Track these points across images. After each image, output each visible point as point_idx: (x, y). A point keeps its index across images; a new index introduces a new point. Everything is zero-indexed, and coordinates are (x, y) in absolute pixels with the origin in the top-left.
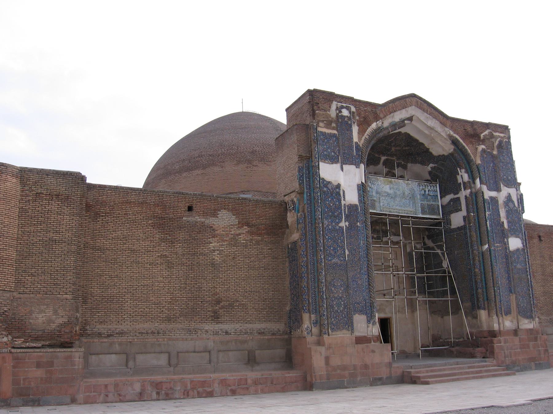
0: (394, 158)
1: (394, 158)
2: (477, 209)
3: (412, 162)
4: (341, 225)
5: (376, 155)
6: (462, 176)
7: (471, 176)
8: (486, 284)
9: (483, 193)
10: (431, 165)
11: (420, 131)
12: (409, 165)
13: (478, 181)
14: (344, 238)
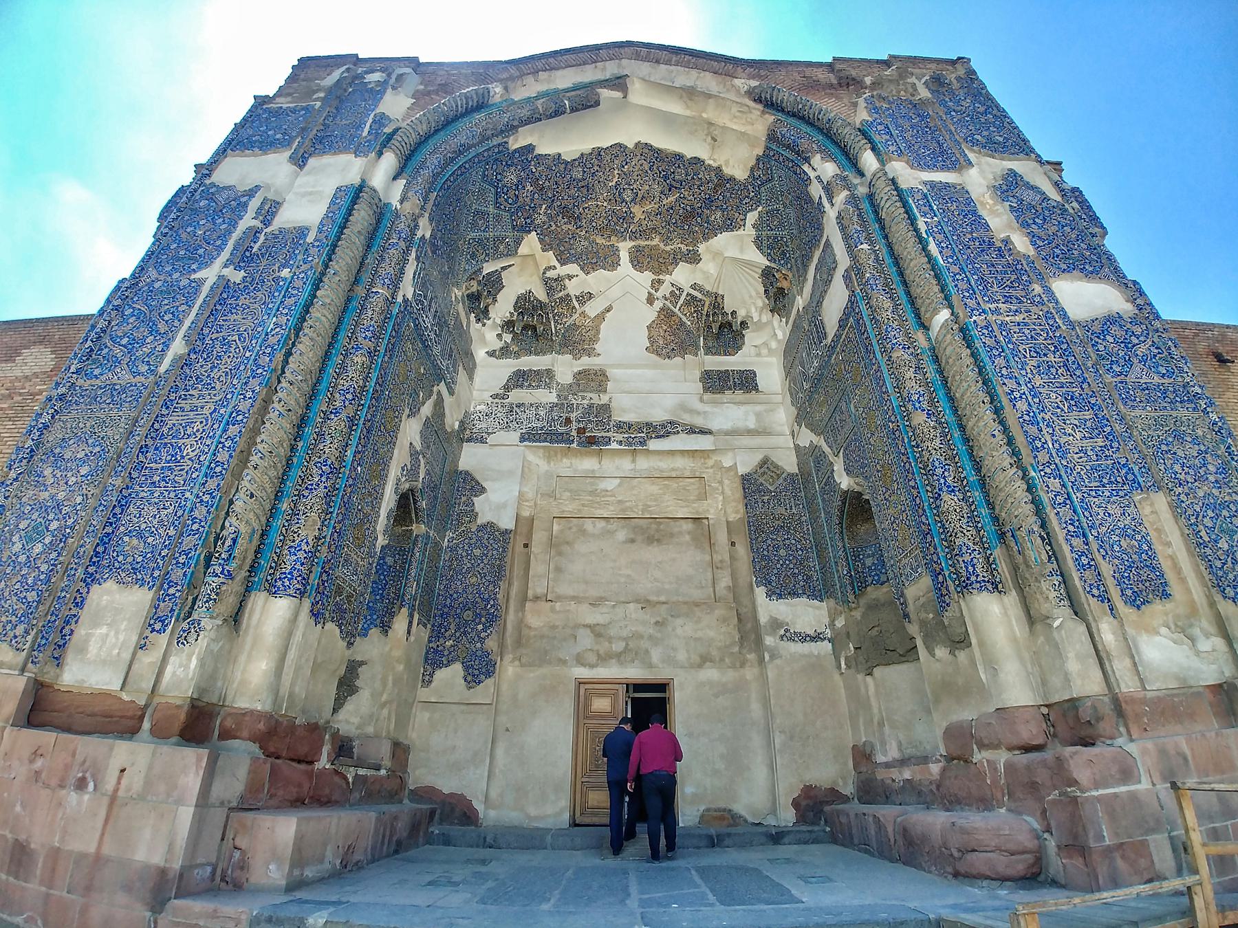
0: (656, 241)
1: (656, 241)
3: (706, 238)
5: (600, 240)
6: (818, 178)
7: (845, 162)
8: (978, 466)
10: (752, 217)
12: (702, 248)
13: (869, 161)
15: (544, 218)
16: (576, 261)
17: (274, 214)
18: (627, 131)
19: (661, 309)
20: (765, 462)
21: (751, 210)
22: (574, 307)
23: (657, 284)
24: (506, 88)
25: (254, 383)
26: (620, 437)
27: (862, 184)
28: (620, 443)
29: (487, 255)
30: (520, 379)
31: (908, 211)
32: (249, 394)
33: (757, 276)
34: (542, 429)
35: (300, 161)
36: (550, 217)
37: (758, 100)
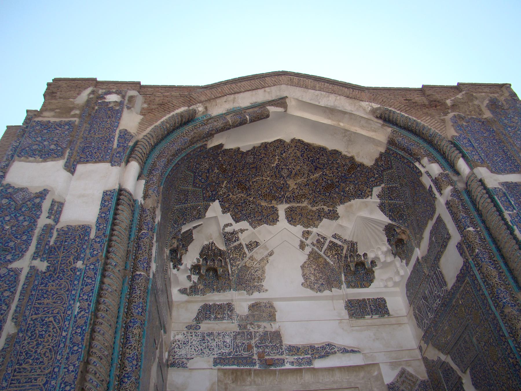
0: (305, 204)
1: (305, 204)
2: (480, 215)
3: (342, 202)
4: (15, 265)
5: (264, 204)
6: (427, 173)
9: (481, 181)
10: (377, 190)
11: (315, 126)
12: (341, 209)
13: (462, 165)
14: (13, 293)
15: (224, 190)
16: (246, 219)
17: (59, 212)
18: (287, 133)
19: (311, 253)
20: (403, 373)
21: (376, 186)
22: (245, 253)
23: (307, 234)
24: (206, 108)
25: (73, 358)
26: (291, 359)
27: (459, 181)
28: (292, 363)
29: (185, 219)
30: (207, 312)
31: (496, 205)
32: (71, 368)
33: (381, 229)
34: (230, 354)
35: (71, 168)
36: (228, 189)
37: (380, 118)
